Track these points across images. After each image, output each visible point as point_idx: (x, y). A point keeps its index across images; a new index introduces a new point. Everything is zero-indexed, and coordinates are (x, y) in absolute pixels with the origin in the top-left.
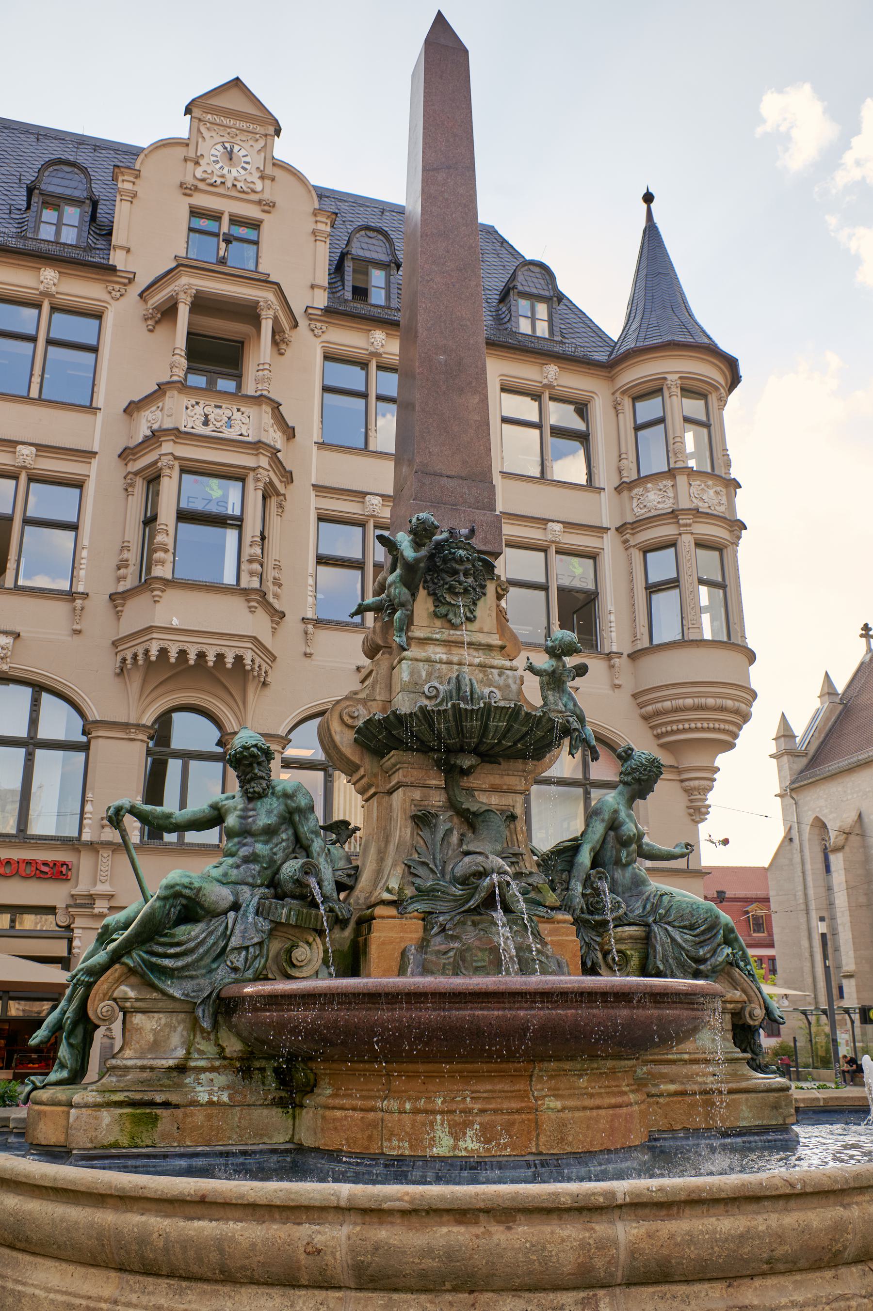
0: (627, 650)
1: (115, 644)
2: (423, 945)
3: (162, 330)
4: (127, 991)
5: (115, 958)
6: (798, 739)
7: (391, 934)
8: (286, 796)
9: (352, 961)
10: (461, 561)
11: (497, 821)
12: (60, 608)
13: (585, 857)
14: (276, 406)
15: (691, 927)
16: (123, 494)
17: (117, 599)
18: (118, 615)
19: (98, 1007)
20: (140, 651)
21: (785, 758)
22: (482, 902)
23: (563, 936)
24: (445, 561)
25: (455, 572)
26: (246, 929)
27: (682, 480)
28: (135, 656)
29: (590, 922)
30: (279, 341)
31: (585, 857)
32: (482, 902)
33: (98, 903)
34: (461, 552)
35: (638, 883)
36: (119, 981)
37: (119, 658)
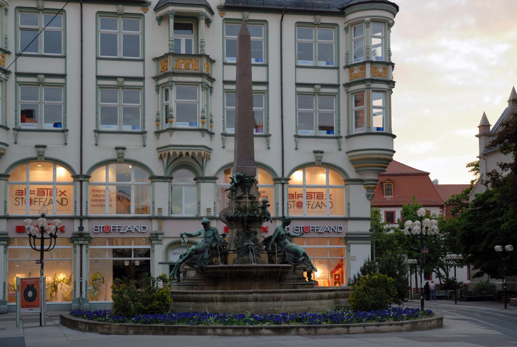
0: (346, 135)
1: (158, 149)
2: (238, 258)
3: (164, 24)
4: (186, 267)
5: (184, 261)
6: (491, 128)
7: (232, 257)
8: (213, 230)
9: (225, 262)
10: (246, 180)
11: (252, 234)
12: (139, 137)
13: (273, 239)
14: (207, 57)
15: (294, 253)
16: (156, 93)
17: (158, 133)
18: (158, 138)
19: (181, 270)
20: (167, 153)
21: (483, 137)
22: (247, 250)
23: (264, 256)
24: (244, 180)
25: (245, 183)
26: (206, 255)
27: (368, 66)
28: (165, 154)
29: (271, 254)
30: (208, 22)
31: (273, 239)
32: (247, 250)
33: (159, 236)
34: (247, 179)
35: (285, 243)
36: (185, 265)
37: (159, 154)
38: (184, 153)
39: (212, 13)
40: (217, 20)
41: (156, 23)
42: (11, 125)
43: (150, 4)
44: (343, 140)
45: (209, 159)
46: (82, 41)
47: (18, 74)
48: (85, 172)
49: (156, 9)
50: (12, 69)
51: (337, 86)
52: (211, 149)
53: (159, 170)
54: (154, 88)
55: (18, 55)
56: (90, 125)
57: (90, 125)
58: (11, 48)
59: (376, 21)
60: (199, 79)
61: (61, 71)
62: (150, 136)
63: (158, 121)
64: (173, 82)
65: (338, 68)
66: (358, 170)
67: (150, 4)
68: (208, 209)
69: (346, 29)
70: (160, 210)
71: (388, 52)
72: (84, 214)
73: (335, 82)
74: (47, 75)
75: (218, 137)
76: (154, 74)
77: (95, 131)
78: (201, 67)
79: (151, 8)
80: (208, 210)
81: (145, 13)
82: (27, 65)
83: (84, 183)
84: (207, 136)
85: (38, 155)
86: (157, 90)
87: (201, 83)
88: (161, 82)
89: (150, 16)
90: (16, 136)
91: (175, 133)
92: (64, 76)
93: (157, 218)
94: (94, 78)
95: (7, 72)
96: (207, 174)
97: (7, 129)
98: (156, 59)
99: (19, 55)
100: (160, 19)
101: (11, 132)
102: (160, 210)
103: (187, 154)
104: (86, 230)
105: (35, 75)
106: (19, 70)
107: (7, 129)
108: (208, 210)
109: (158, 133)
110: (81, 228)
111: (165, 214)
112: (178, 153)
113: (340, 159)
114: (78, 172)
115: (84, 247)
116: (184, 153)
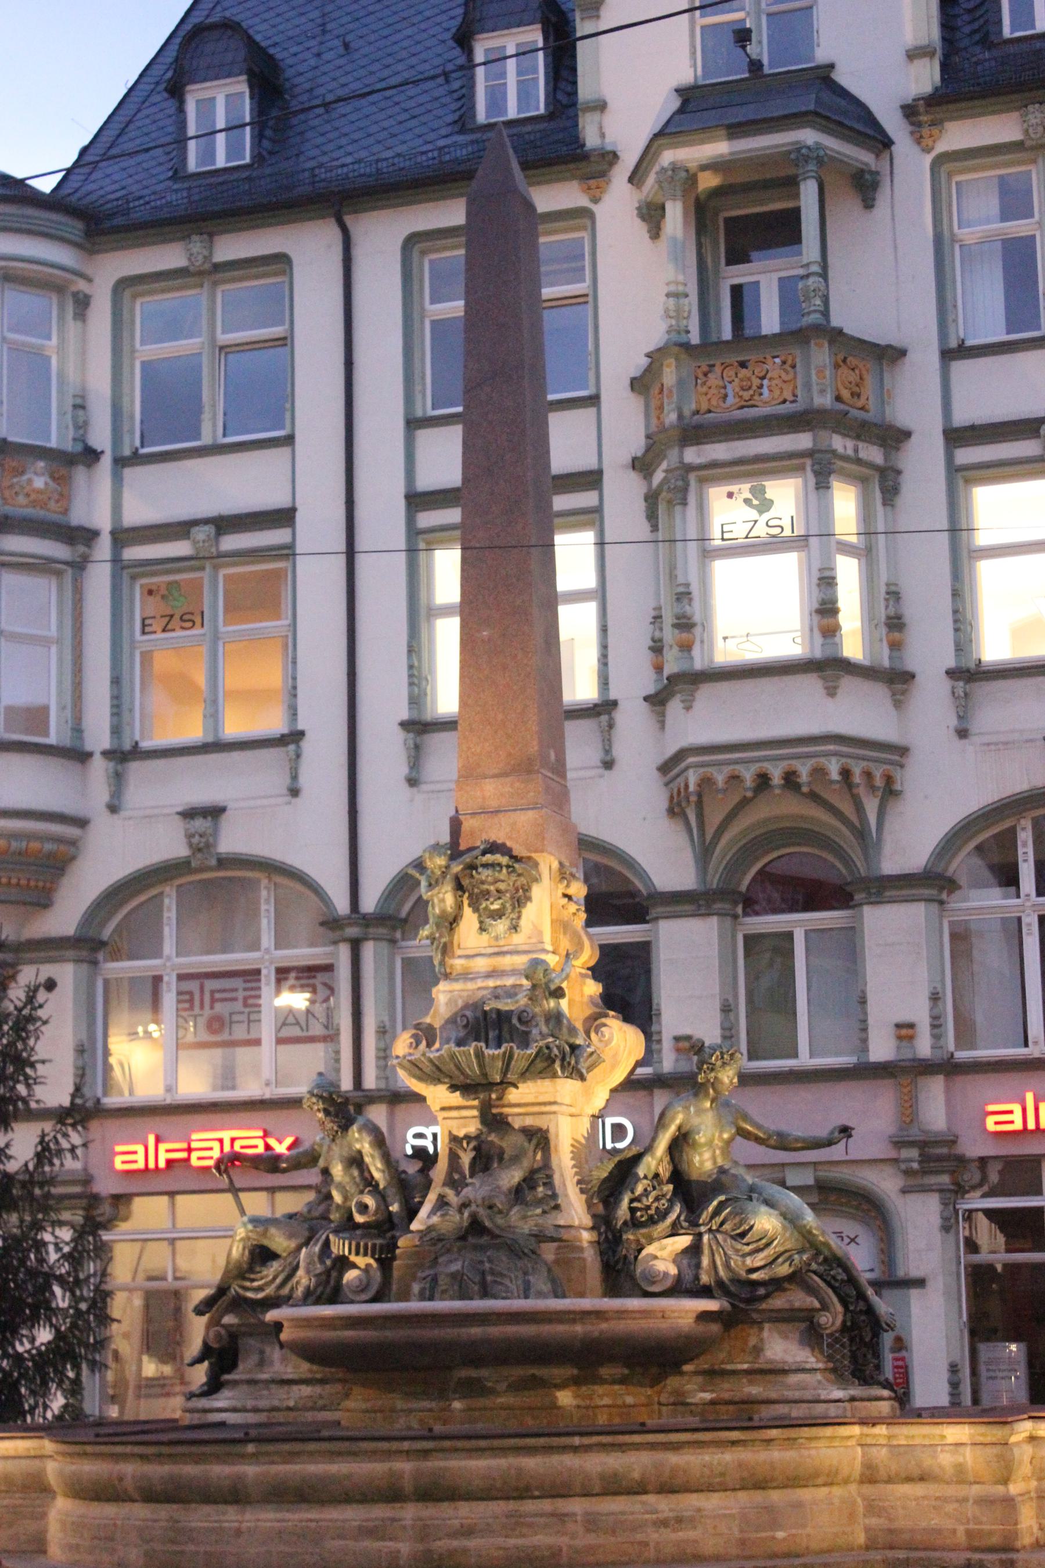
38: (776, 775)
39: (882, 143)
40: (911, 165)
41: (641, 229)
42: (98, 736)
43: (611, 157)
45: (890, 792)
47: (122, 536)
48: (369, 903)
50: (102, 520)
52: (903, 751)
53: (666, 861)
55: (121, 462)
58: (101, 437)
60: (803, 441)
61: (277, 499)
63: (657, 648)
64: (690, 468)
67: (611, 157)
68: (898, 1026)
72: (370, 1082)
74: (224, 524)
75: (933, 694)
76: (636, 445)
77: (405, 725)
78: (808, 386)
80: (905, 1031)
81: (596, 200)
82: (158, 495)
83: (369, 951)
84: (880, 692)
85: (190, 845)
87: (809, 454)
90: (118, 780)
91: (705, 693)
94: (400, 505)
95: (90, 535)
96: (891, 865)
97: (78, 755)
99: (137, 459)
101: (99, 766)
103: (790, 779)
105: (181, 529)
107: (78, 755)
108: (905, 1031)
109: (657, 701)
112: (748, 775)
114: (342, 905)
116: (776, 775)
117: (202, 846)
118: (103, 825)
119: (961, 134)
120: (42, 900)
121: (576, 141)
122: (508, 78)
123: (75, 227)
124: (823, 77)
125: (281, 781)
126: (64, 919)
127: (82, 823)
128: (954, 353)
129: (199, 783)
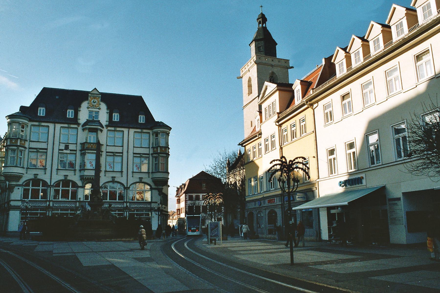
30: (101, 131)
39: (103, 128)
40: (105, 130)
42: (25, 167)
44: (150, 174)
46: (54, 137)
47: (30, 148)
48: (52, 184)
49: (83, 126)
51: (148, 154)
54: (80, 155)
56: (55, 167)
57: (55, 167)
59: (163, 132)
62: (77, 172)
65: (149, 148)
66: (156, 185)
69: (153, 134)
70: (80, 198)
71: (167, 143)
73: (148, 153)
79: (81, 126)
86: (81, 155)
88: (82, 152)
89: (80, 128)
90: (27, 171)
92: (47, 149)
93: (78, 201)
95: (25, 148)
97: (24, 168)
98: (81, 144)
100: (83, 130)
101: (25, 169)
102: (80, 198)
103: (90, 178)
104: (51, 205)
106: (30, 146)
107: (24, 168)
110: (49, 205)
111: (82, 200)
113: (149, 181)
115: (50, 212)
117: (35, 177)
118: (26, 175)
119: (109, 128)
120: (18, 181)
121: (77, 121)
122: (70, 114)
123: (28, 119)
124: (99, 121)
125: (73, 174)
126: (21, 182)
127: (23, 174)
128: (107, 145)
129: (35, 172)
